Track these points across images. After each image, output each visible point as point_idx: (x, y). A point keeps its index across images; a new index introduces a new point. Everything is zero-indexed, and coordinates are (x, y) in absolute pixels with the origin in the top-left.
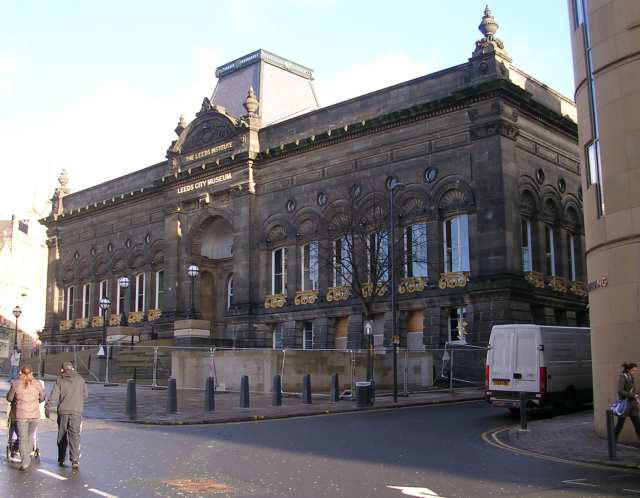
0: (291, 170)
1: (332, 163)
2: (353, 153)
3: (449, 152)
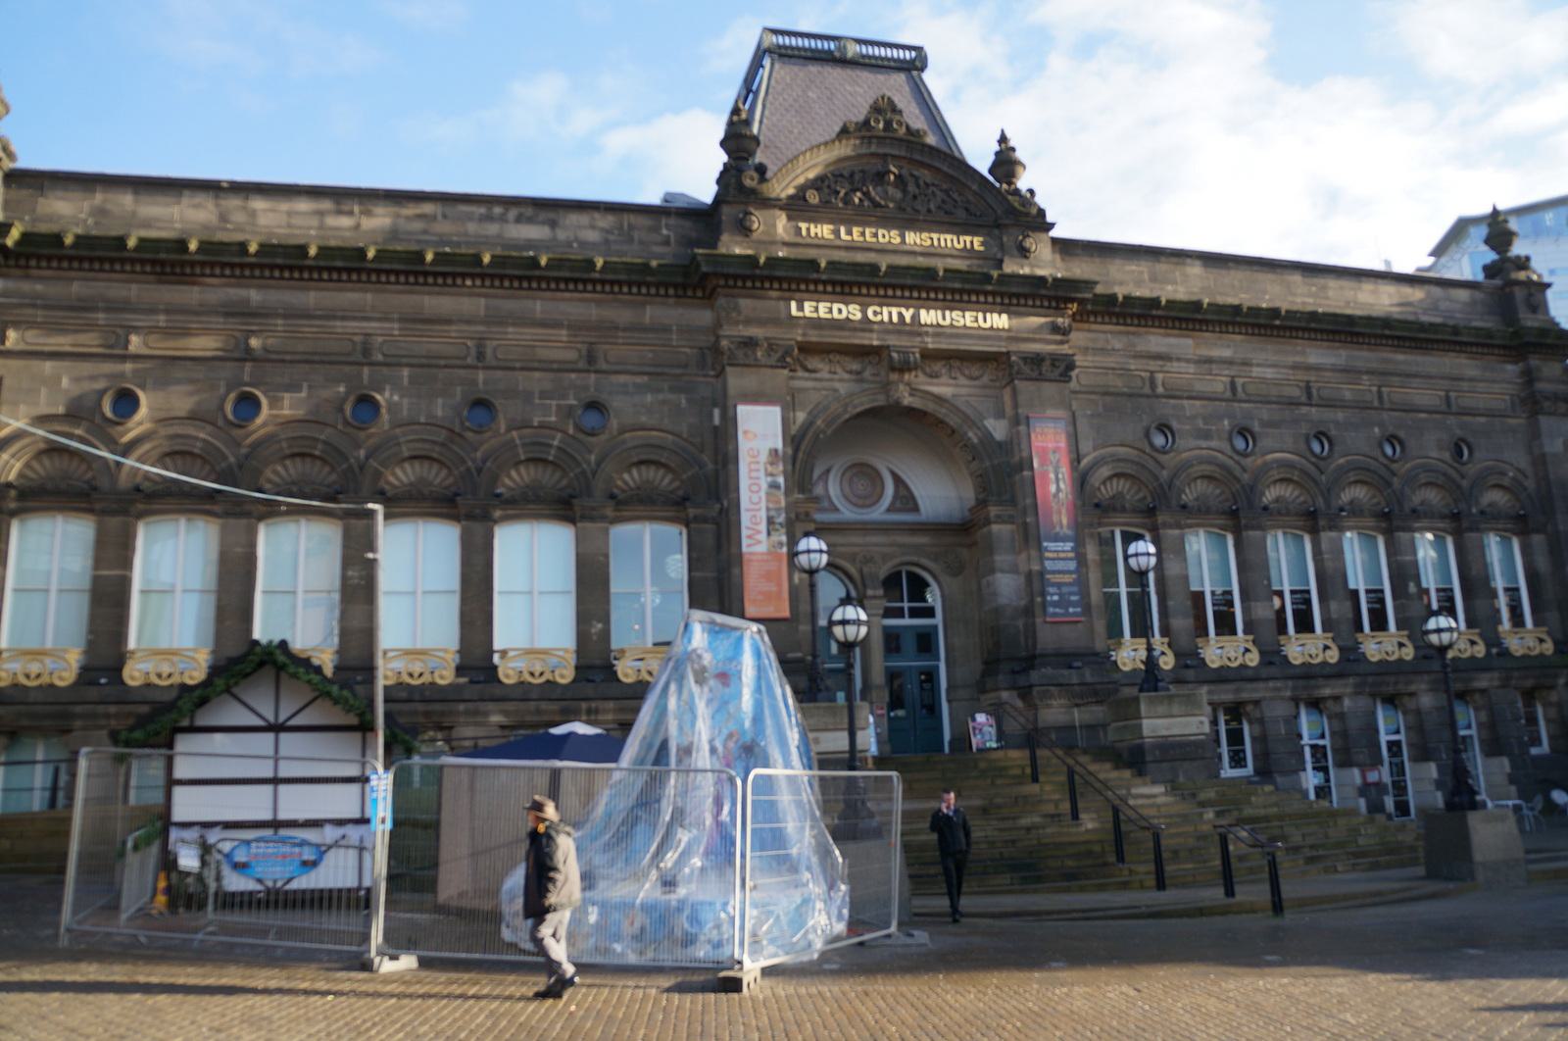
0: (1158, 357)
1: (1256, 371)
2: (1308, 368)
3: (1482, 420)
